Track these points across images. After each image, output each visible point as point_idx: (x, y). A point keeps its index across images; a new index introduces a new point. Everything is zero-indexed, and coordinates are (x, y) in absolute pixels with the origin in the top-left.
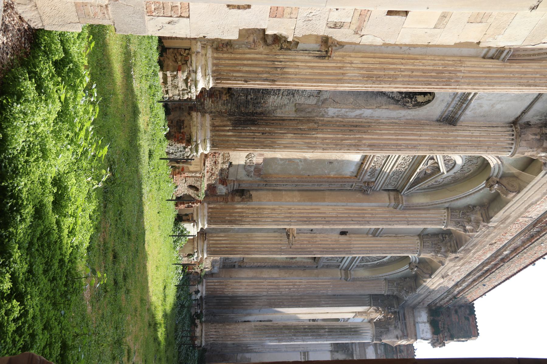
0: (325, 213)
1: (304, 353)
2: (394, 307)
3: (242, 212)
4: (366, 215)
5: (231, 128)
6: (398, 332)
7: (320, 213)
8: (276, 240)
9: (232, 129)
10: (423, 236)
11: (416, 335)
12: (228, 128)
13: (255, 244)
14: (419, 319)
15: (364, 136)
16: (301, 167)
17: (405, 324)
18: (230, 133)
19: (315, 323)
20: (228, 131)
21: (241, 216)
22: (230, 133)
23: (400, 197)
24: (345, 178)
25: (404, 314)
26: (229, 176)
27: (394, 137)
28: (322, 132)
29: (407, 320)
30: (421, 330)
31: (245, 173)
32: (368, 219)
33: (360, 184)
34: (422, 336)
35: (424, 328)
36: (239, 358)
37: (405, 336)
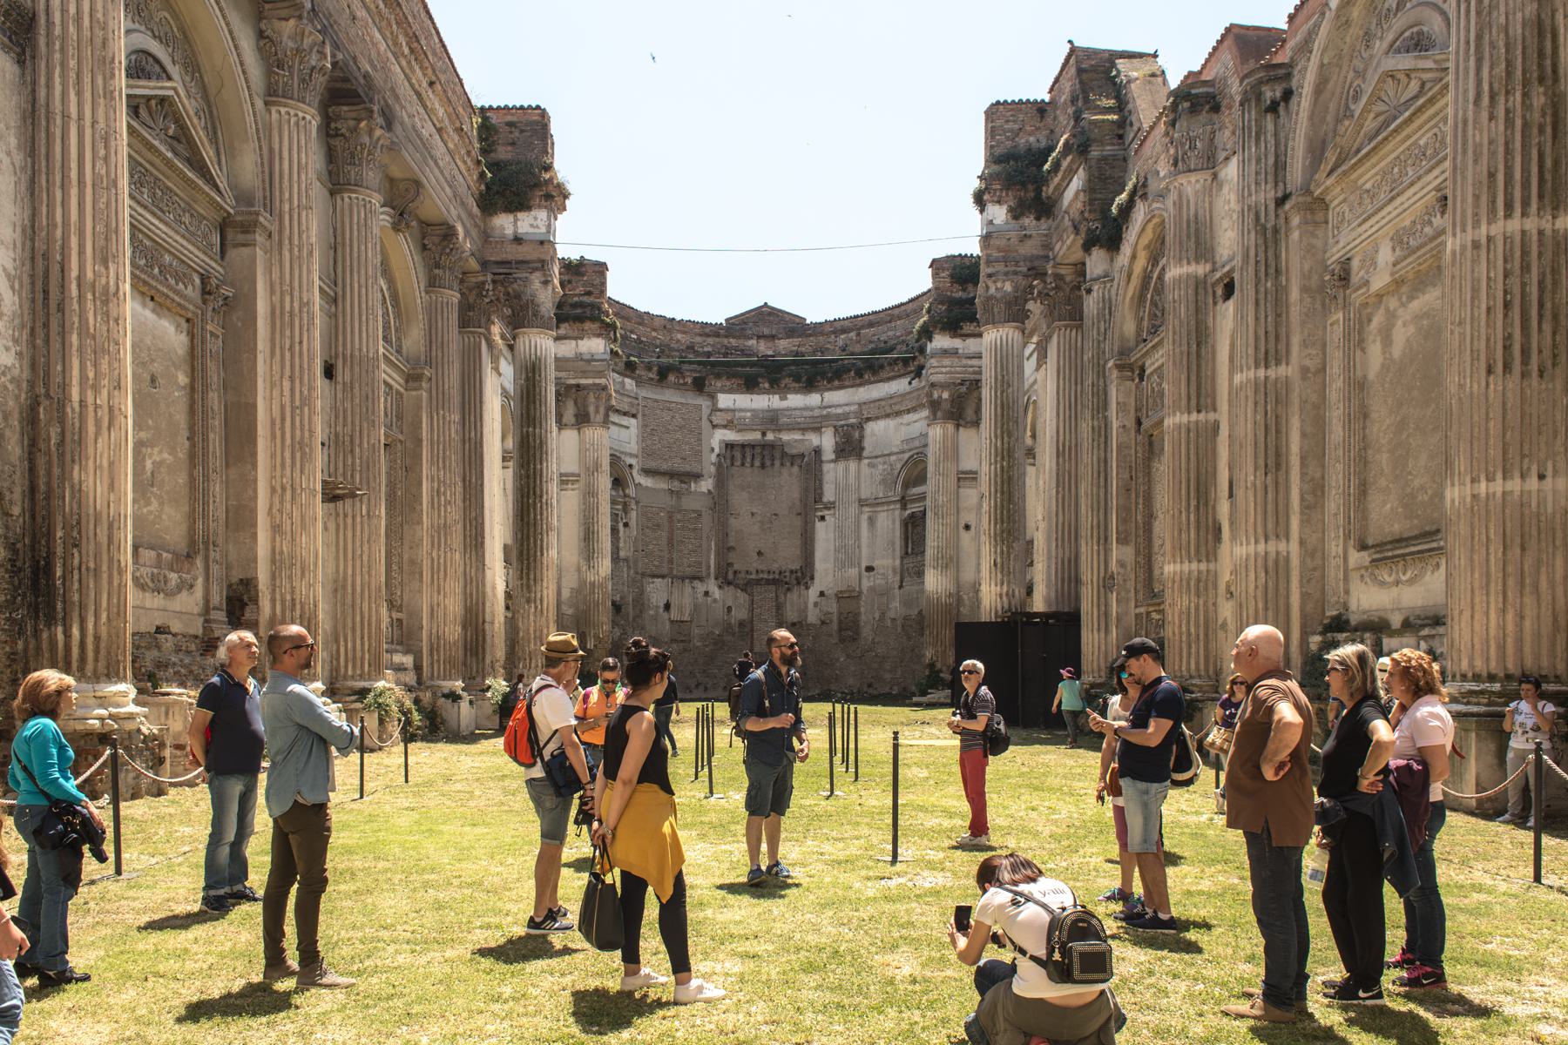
0: (283, 407)
1: (562, 482)
2: (483, 283)
3: (283, 601)
4: (288, 308)
5: (60, 629)
6: (536, 279)
7: (283, 419)
8: (345, 528)
9: (64, 625)
10: (337, 181)
11: (542, 243)
12: (60, 637)
13: (354, 575)
14: (509, 231)
15: (74, 273)
16: (166, 455)
17: (518, 262)
18: (76, 632)
19: (515, 454)
20: (67, 635)
21: (294, 605)
22: (76, 632)
23: (239, 218)
24: (192, 347)
25: (497, 263)
26: (192, 632)
27: (74, 192)
28: (64, 386)
29: (510, 257)
30: (531, 230)
31: (184, 593)
32: (296, 305)
33: (210, 313)
34: (543, 230)
35: (528, 223)
36: (570, 612)
37: (542, 265)
